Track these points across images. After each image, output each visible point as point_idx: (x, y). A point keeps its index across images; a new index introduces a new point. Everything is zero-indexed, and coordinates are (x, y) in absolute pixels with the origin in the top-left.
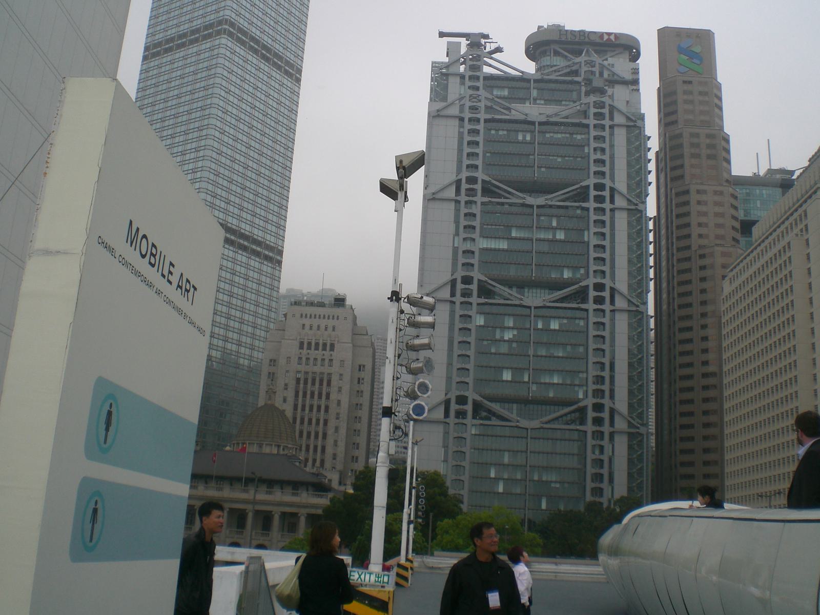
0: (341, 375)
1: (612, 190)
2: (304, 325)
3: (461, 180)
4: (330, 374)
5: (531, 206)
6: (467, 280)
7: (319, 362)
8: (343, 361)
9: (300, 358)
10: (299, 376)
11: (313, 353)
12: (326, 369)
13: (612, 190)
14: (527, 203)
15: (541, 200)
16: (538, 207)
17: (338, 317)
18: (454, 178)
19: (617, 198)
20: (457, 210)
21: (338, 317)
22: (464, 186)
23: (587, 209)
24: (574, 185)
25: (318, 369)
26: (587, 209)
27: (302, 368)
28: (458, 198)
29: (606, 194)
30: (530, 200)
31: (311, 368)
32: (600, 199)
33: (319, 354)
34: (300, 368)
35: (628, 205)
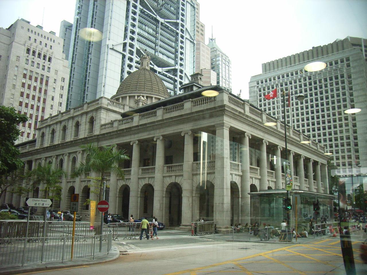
0: (55, 80)
2: (30, 37)
4: (48, 77)
6: (131, 46)
7: (41, 67)
8: (57, 71)
9: (27, 60)
10: (25, 72)
11: (37, 60)
12: (45, 73)
17: (54, 41)
21: (54, 41)
24: (170, 19)
25: (40, 71)
27: (29, 67)
30: (158, 18)
31: (35, 69)
33: (41, 61)
34: (26, 67)
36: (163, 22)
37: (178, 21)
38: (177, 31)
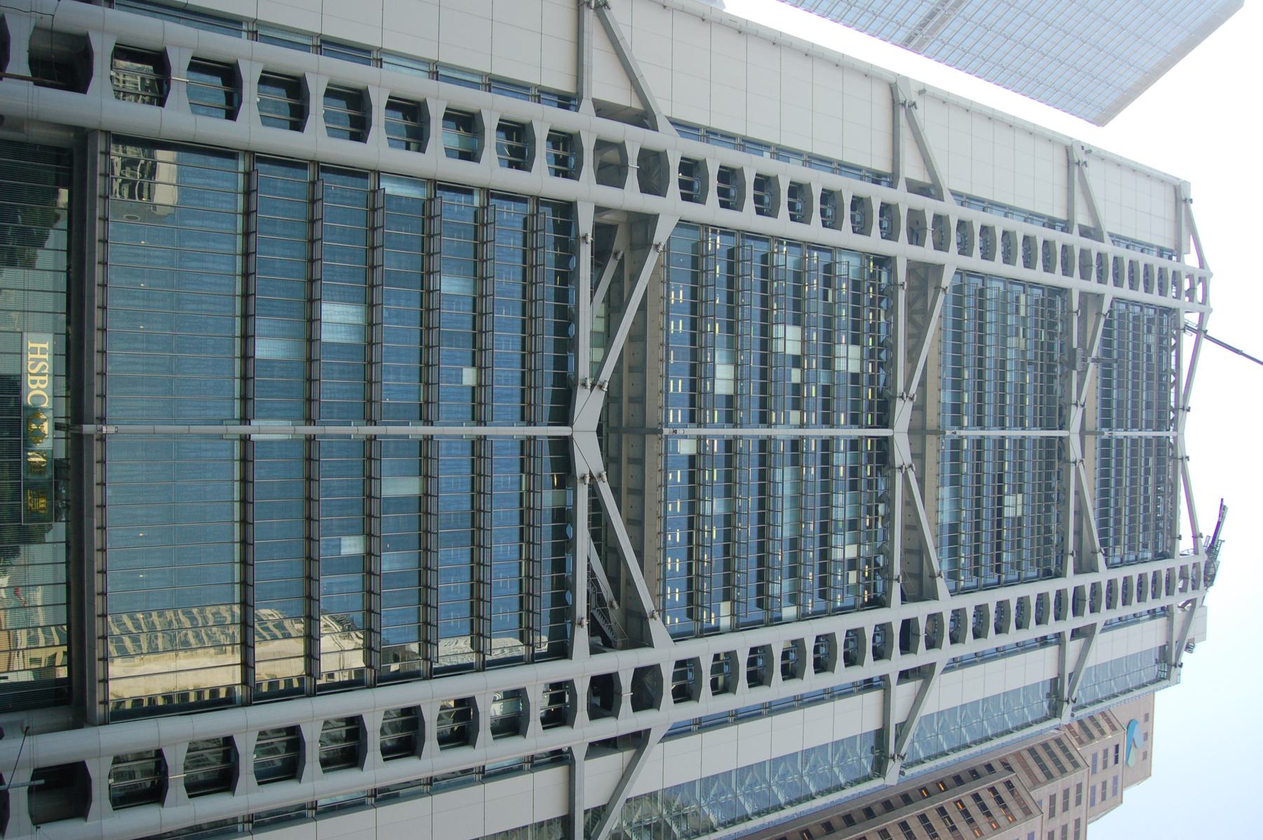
1: (637, 740)
3: (655, 128)
5: (563, 414)
13: (637, 740)
14: (582, 396)
15: (588, 457)
16: (563, 448)
18: (663, 108)
19: (615, 761)
20: (541, 95)
22: (634, 139)
23: (561, 650)
26: (561, 650)
28: (587, 106)
29: (627, 721)
30: (589, 407)
32: (604, 692)
35: (586, 812)
36: (581, 468)
37: (657, 629)
38: (581, 638)
